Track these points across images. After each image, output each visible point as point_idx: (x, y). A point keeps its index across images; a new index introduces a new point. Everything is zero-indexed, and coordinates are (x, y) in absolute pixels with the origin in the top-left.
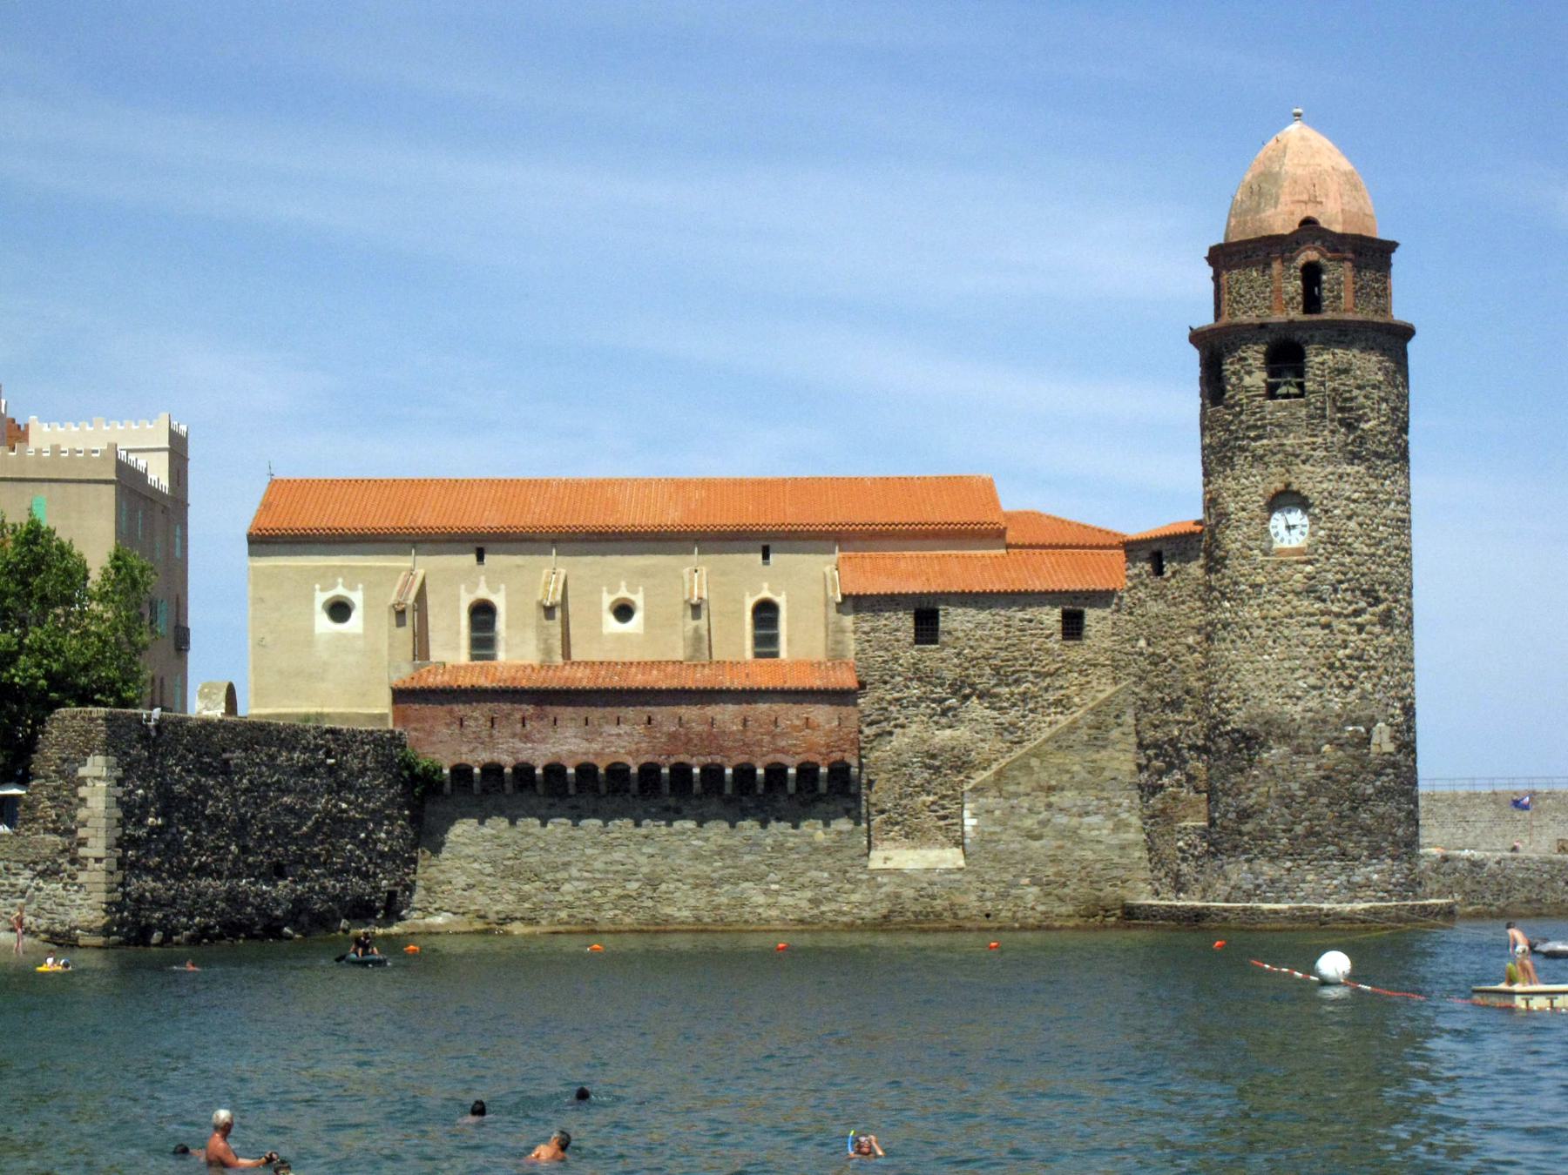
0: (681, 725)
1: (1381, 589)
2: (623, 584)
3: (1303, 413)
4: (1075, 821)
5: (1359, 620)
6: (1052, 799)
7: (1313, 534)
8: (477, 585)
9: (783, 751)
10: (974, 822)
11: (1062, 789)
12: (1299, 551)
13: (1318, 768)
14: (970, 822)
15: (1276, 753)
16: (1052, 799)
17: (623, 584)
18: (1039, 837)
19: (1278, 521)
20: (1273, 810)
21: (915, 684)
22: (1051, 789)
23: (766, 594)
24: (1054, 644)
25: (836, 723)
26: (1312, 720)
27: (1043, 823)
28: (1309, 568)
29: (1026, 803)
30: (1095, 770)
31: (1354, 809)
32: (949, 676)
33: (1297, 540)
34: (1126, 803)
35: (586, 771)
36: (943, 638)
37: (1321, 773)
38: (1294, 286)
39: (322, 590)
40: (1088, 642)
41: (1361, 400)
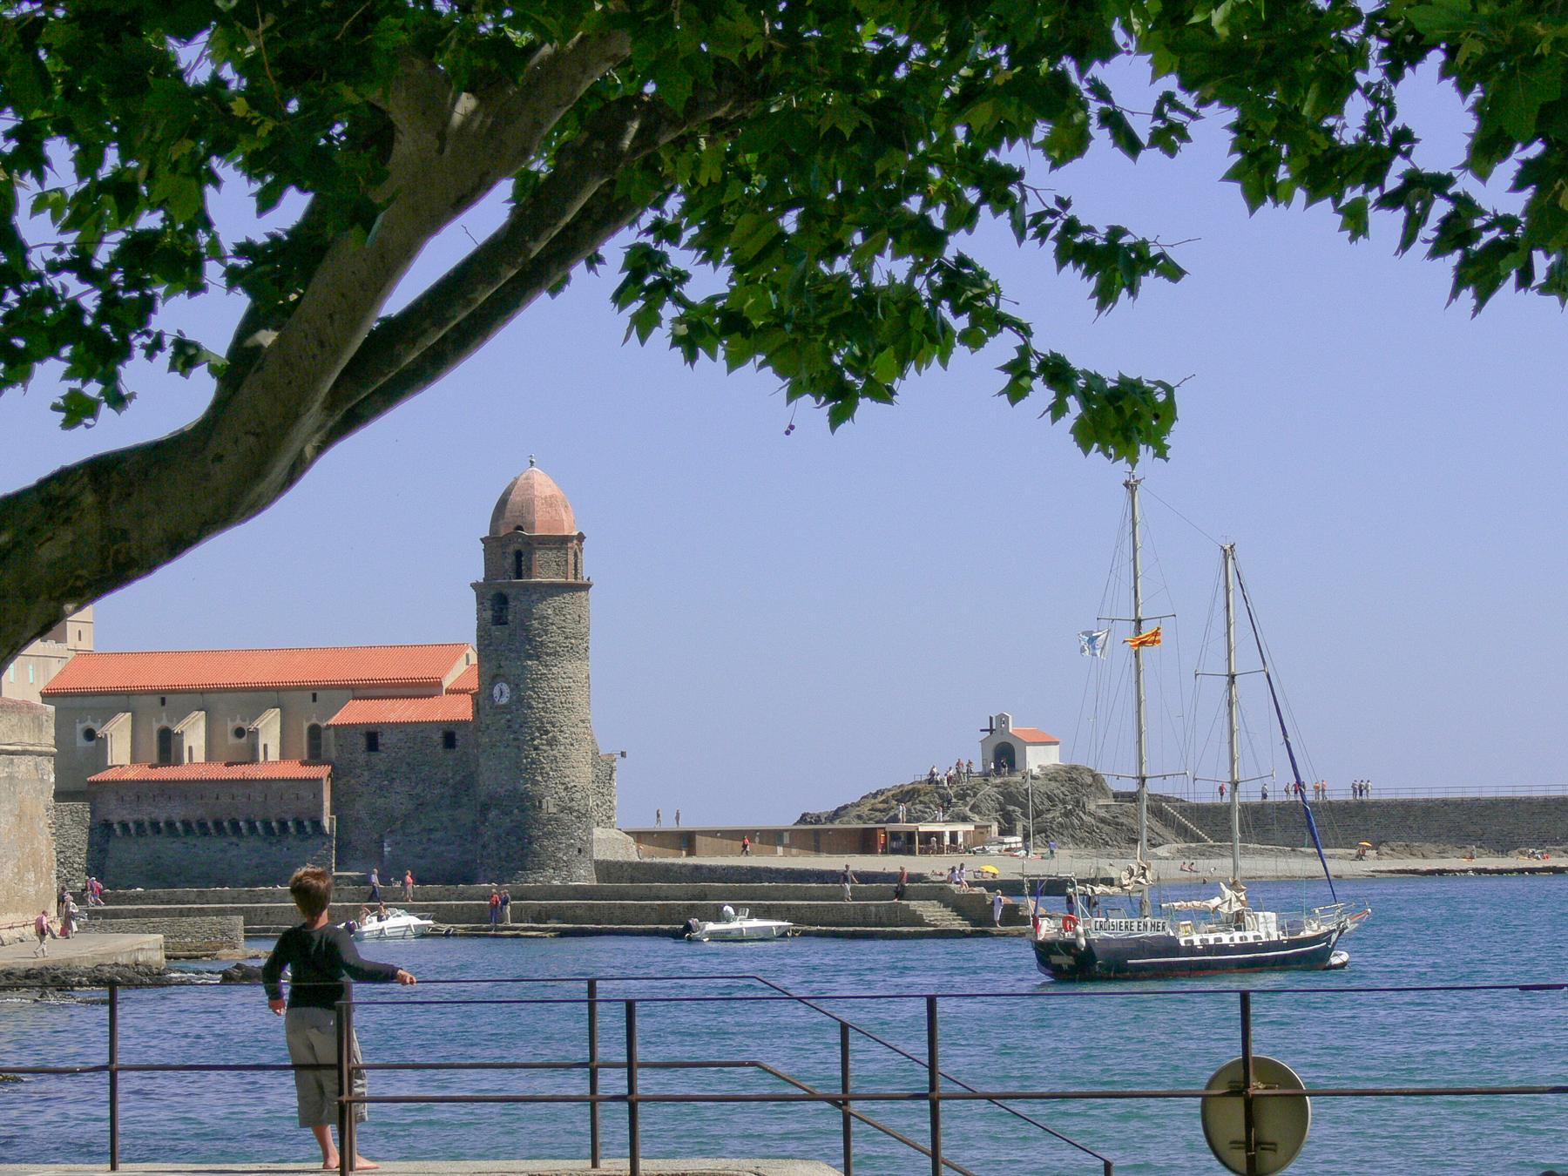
0: (233, 798)
1: (549, 727)
2: (238, 716)
3: (507, 632)
4: (442, 848)
5: (535, 743)
6: (432, 837)
7: (511, 697)
8: (162, 719)
9: (286, 812)
10: (389, 849)
11: (437, 830)
12: (504, 706)
13: (512, 821)
14: (387, 849)
15: (493, 814)
16: (432, 837)
17: (238, 716)
18: (421, 858)
19: (496, 691)
20: (493, 845)
21: (366, 773)
22: (431, 830)
23: (314, 721)
24: (440, 749)
25: (312, 796)
26: (509, 796)
27: (425, 849)
28: (509, 717)
29: (416, 838)
30: (453, 820)
31: (530, 843)
32: (383, 769)
33: (504, 700)
34: (470, 838)
35: (187, 824)
36: (380, 748)
37: (514, 824)
38: (511, 560)
39: (80, 722)
40: (457, 749)
41: (536, 625)
